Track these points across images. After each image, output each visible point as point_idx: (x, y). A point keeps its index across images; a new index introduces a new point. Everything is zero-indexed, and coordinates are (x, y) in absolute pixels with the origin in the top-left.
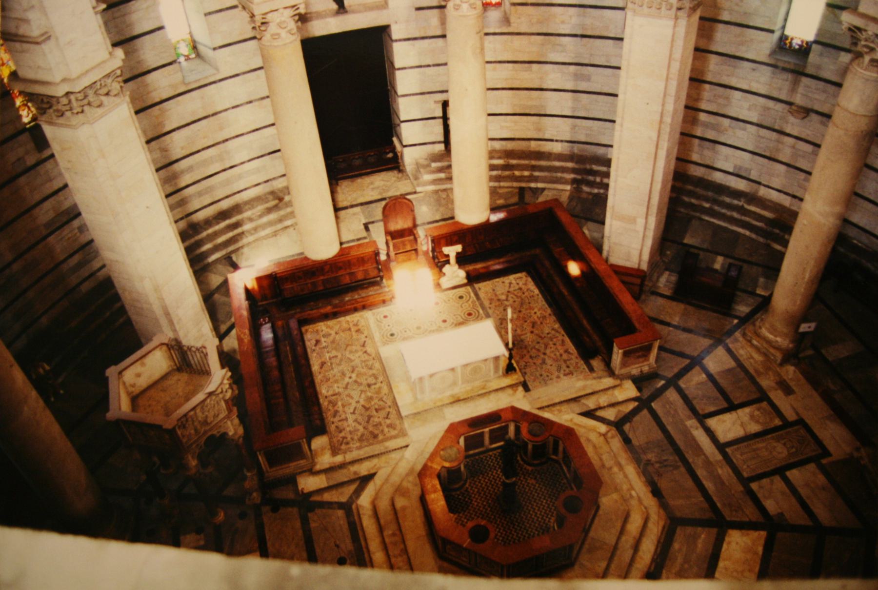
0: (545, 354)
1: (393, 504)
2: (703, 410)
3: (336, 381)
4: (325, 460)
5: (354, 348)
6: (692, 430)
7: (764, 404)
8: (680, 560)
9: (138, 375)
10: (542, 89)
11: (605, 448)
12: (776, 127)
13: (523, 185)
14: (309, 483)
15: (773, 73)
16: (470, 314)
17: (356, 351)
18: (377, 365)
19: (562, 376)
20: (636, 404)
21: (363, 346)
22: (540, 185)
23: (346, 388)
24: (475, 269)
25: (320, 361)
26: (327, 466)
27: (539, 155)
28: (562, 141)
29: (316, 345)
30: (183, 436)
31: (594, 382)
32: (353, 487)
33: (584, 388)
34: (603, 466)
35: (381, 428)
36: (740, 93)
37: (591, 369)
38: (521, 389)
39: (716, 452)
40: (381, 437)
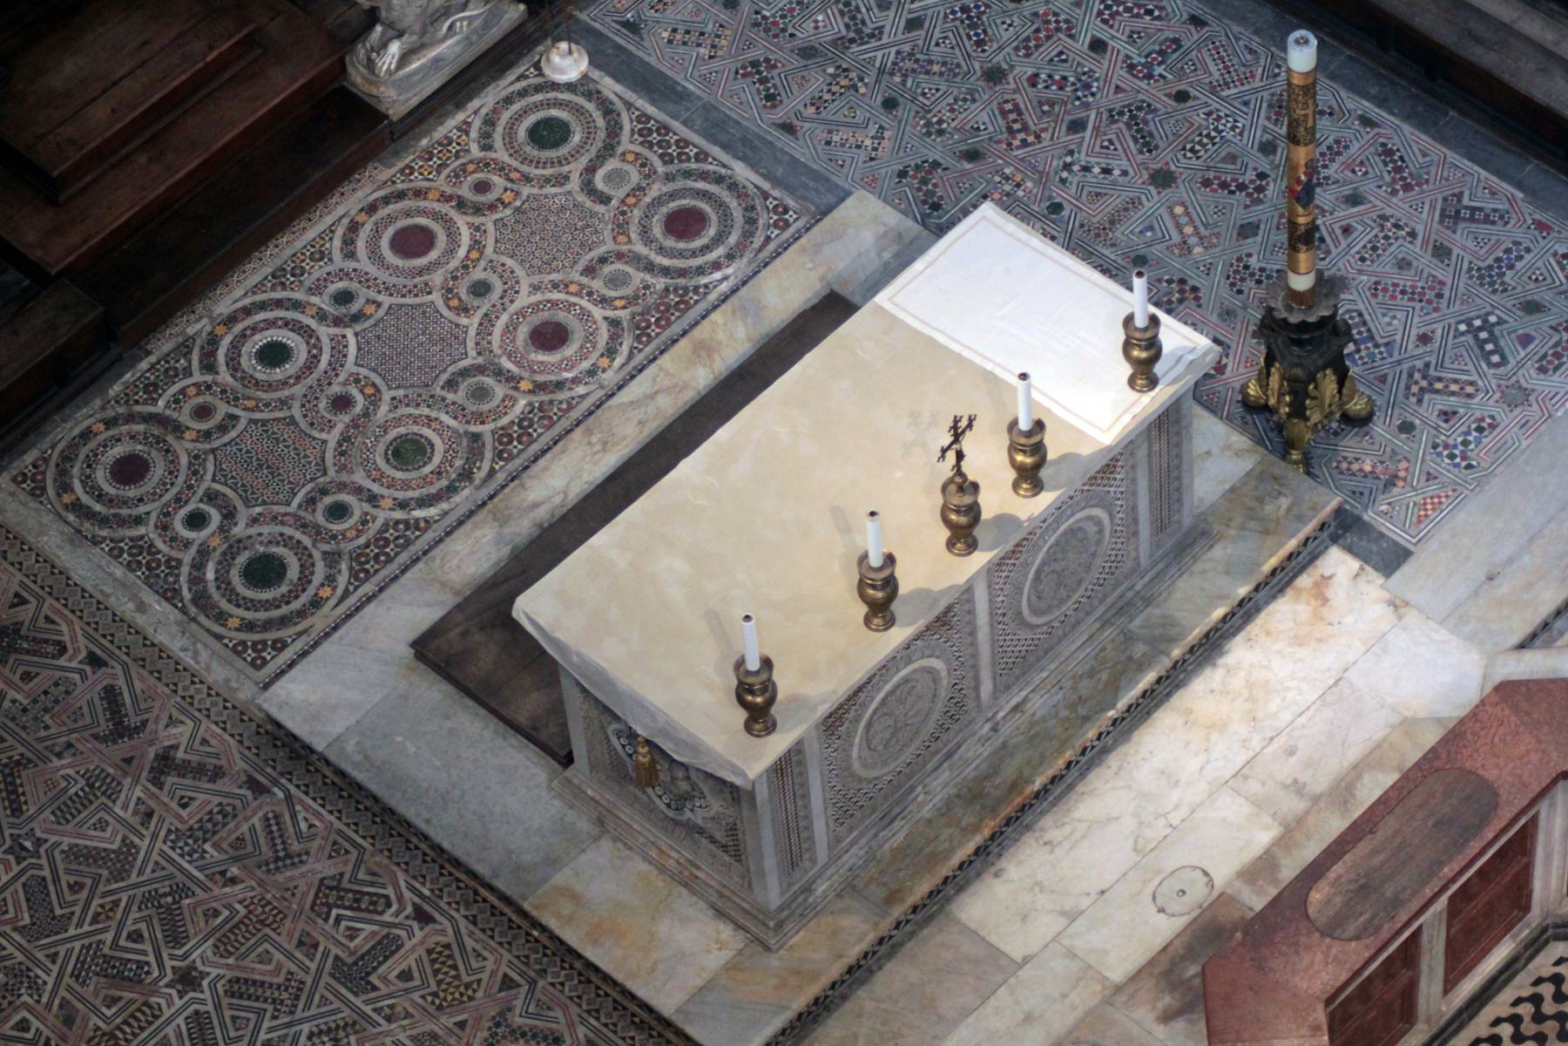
16: (684, 224)
17: (100, 787)
18: (313, 816)
19: (1529, 377)
21: (121, 730)
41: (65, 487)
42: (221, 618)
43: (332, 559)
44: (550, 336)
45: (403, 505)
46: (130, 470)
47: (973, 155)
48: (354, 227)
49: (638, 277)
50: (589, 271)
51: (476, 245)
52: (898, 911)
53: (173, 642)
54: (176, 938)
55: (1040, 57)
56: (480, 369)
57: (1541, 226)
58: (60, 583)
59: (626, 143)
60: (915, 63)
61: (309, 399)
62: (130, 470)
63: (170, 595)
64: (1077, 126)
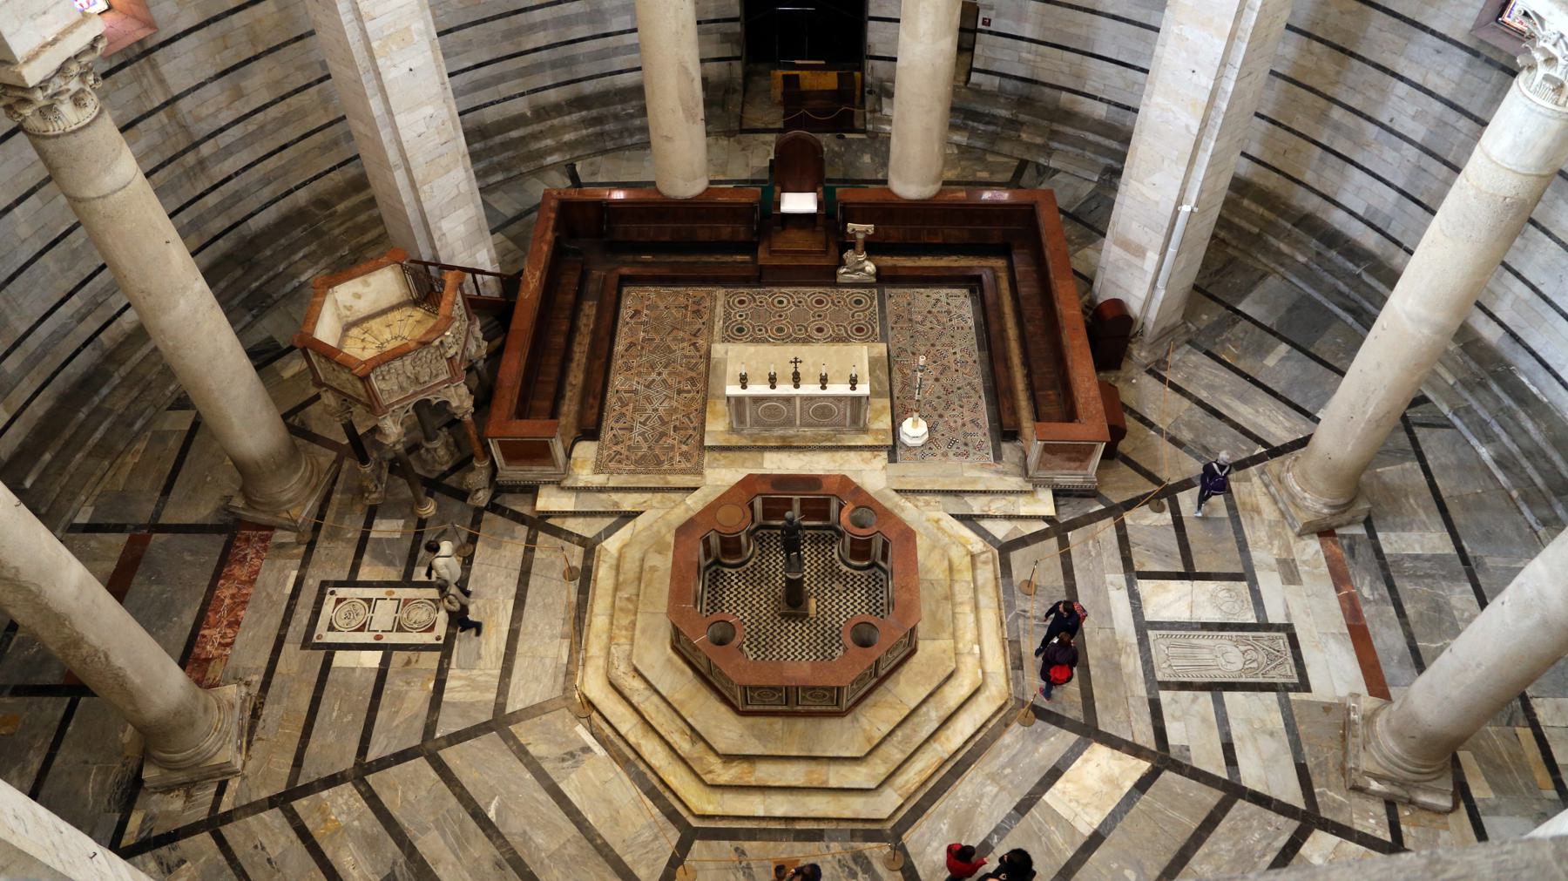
0: (941, 416)
1: (643, 560)
2: (1143, 565)
3: (639, 374)
4: (584, 475)
5: (681, 334)
6: (1110, 588)
7: (1243, 586)
8: (1003, 758)
9: (358, 296)
10: (1093, 12)
11: (968, 576)
12: (1450, 159)
14: (549, 501)
15: (1470, 65)
16: (860, 330)
17: (683, 340)
18: (702, 367)
20: (1044, 526)
22: (1053, 164)
23: (648, 387)
24: (895, 267)
26: (581, 484)
27: (1069, 116)
28: (1109, 102)
30: (382, 391)
31: (994, 476)
32: (609, 521)
33: (975, 481)
34: (950, 597)
36: (1407, 87)
37: (998, 457)
38: (884, 455)
39: (1132, 630)
40: (666, 467)
44: (820, 330)
46: (741, 302)
53: (716, 329)
58: (713, 310)
60: (924, 334)
62: (741, 302)
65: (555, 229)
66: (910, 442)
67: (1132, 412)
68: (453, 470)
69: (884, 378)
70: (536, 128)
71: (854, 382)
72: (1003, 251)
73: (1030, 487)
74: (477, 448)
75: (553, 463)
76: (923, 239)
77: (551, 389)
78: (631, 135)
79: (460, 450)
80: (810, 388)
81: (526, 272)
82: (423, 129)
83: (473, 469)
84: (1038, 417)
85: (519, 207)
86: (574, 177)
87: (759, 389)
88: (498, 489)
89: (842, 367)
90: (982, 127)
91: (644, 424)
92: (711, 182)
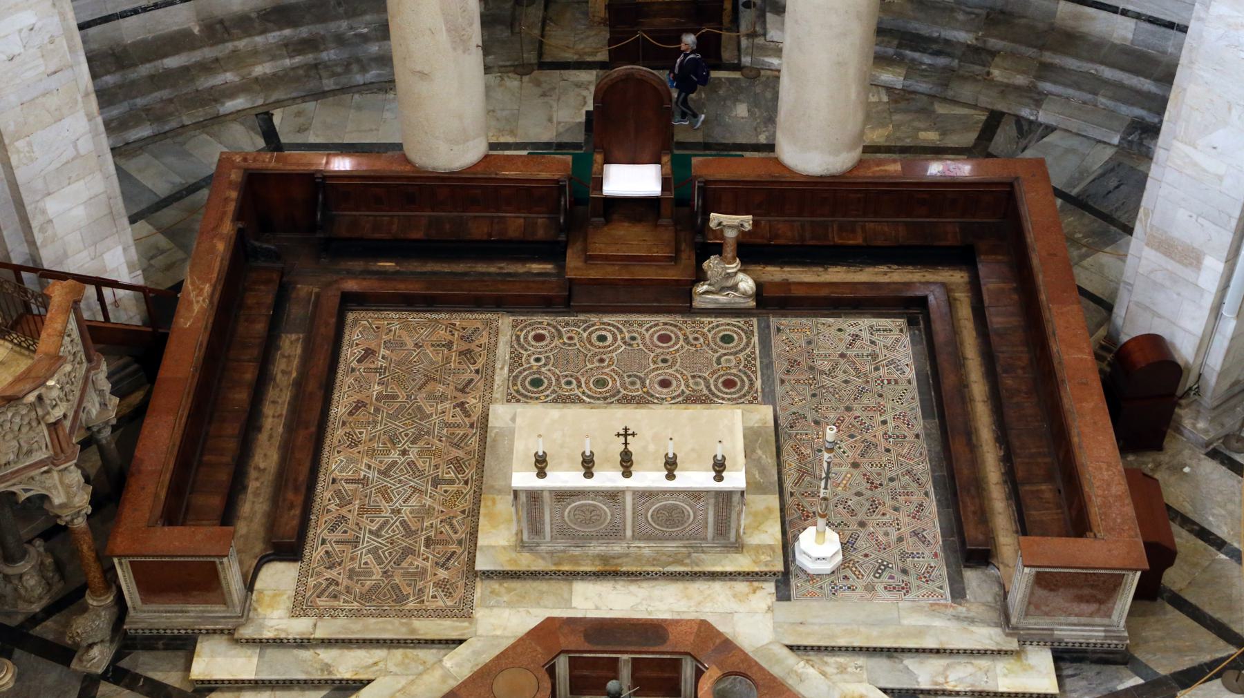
0: (862, 524)
3: (371, 453)
4: (275, 618)
5: (441, 388)
13: (1001, 106)
16: (729, 384)
17: (443, 398)
18: (474, 443)
22: (1043, 117)
23: (385, 473)
24: (786, 284)
25: (356, 397)
28: (1138, 16)
29: (359, 361)
31: (953, 626)
33: (921, 632)
35: (420, 584)
37: (958, 593)
38: (770, 587)
40: (411, 605)
41: (521, 330)
42: (514, 384)
43: (554, 391)
44: (665, 384)
45: (584, 393)
46: (539, 338)
47: (817, 423)
48: (656, 325)
49: (703, 386)
50: (693, 377)
51: (677, 351)
52: (554, 568)
53: (498, 380)
54: (413, 442)
55: (866, 413)
56: (640, 378)
57: (936, 555)
58: (492, 350)
59: (741, 356)
61: (596, 354)
62: (539, 338)
63: (511, 371)
64: (852, 436)
65: (239, 215)
66: (812, 567)
67: (1186, 521)
68: (49, 612)
69: (769, 460)
70: (208, 53)
71: (719, 467)
72: (963, 257)
73: (1013, 644)
74: (95, 575)
75: (223, 600)
76: (827, 237)
77: (224, 476)
78: (364, 69)
79: (63, 577)
80: (649, 478)
81: (188, 285)
82: (17, 49)
83: (85, 609)
84: (1023, 527)
85: (178, 180)
86: (270, 135)
87: (565, 477)
88: (127, 642)
89: (702, 443)
90: (927, 59)
91: (376, 533)
92: (493, 146)
